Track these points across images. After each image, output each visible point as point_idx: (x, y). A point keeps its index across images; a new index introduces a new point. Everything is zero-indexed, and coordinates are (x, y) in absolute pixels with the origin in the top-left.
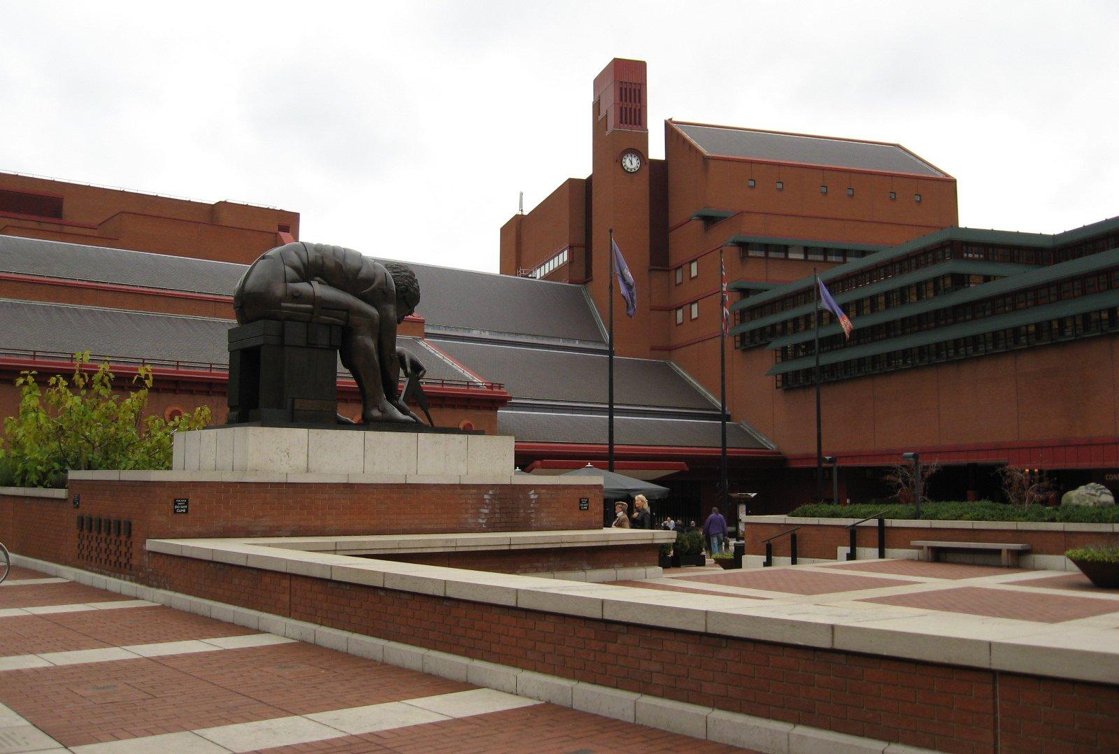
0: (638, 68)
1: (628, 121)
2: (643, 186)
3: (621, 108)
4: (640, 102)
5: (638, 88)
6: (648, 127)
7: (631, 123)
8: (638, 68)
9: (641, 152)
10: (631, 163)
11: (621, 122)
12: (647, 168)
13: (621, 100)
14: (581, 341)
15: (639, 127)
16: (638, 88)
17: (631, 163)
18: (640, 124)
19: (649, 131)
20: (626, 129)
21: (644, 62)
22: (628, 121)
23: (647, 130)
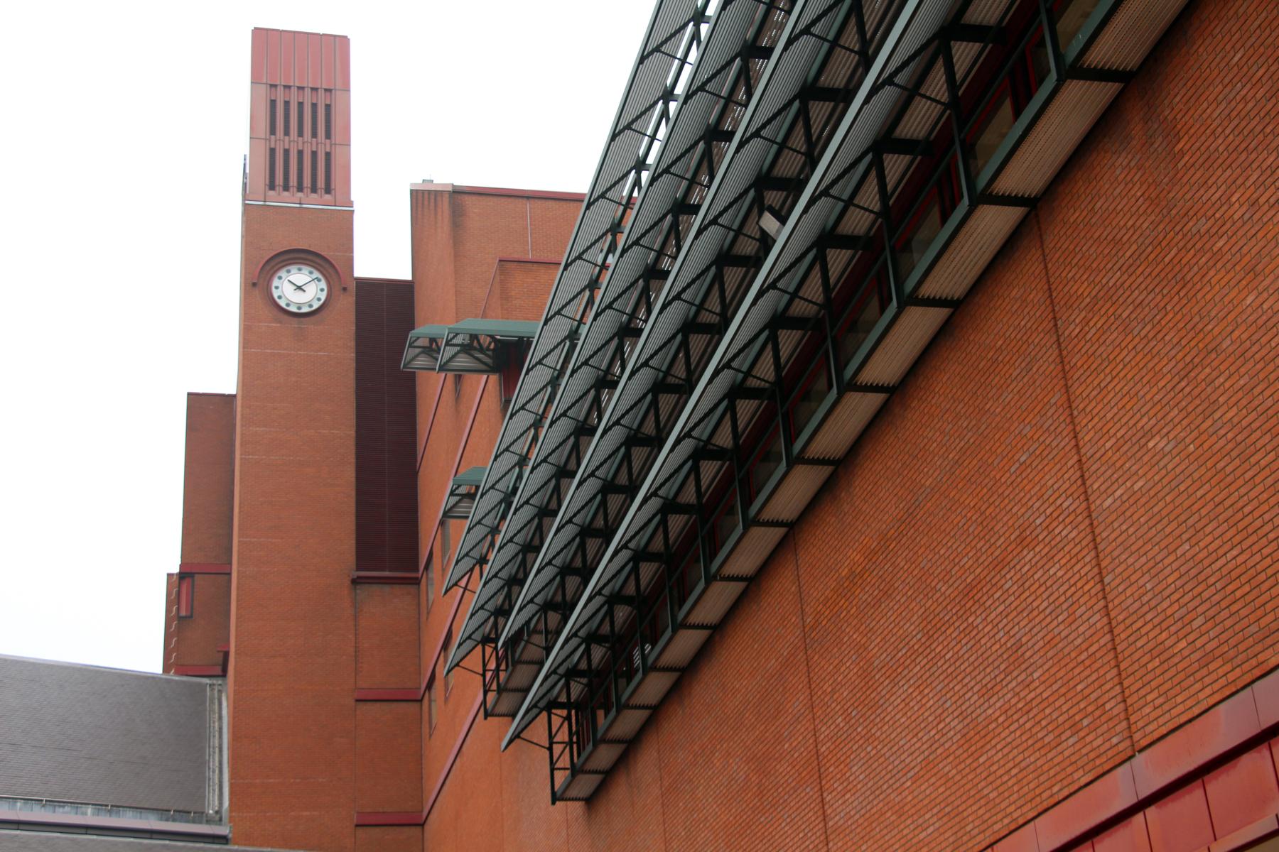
0: (330, 52)
1: (293, 180)
2: (338, 350)
3: (272, 151)
4: (328, 135)
5: (322, 100)
6: (354, 196)
7: (300, 189)
8: (330, 52)
9: (329, 259)
10: (300, 289)
11: (272, 186)
12: (347, 303)
13: (273, 131)
14: (100, 806)
15: (327, 196)
16: (322, 100)
17: (300, 289)
18: (328, 190)
19: (356, 208)
20: (287, 200)
21: (345, 37)
22: (293, 180)
23: (351, 204)
